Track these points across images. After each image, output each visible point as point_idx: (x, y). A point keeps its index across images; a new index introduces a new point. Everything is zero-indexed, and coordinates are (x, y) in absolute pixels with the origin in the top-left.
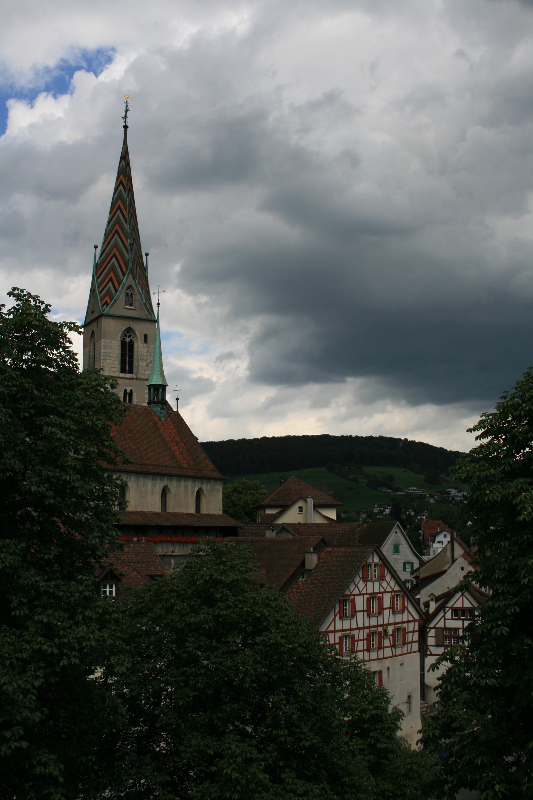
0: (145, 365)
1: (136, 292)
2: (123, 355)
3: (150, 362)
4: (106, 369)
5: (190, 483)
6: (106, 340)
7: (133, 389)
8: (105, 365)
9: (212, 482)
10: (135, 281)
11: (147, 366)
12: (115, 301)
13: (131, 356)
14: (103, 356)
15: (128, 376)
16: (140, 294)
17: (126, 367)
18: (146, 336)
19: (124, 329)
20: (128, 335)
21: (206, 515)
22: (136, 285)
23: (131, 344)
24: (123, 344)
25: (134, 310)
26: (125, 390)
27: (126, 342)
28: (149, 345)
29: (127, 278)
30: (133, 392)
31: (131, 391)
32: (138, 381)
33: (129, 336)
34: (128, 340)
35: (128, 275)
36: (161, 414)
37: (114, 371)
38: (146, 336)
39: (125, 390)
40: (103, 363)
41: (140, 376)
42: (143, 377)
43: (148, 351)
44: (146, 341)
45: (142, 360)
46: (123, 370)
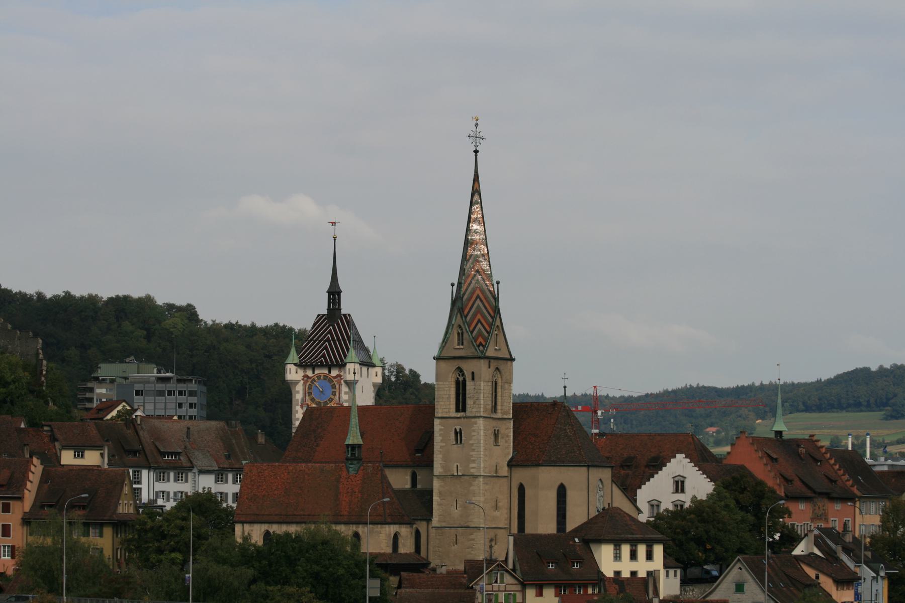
1: (464, 331)
3: (477, 400)
4: (440, 410)
15: (459, 415)
23: (464, 381)
24: (457, 382)
26: (456, 429)
27: (459, 381)
31: (460, 429)
32: (465, 419)
34: (461, 379)
35: (457, 314)
39: (456, 429)
41: (468, 414)
42: (471, 415)
43: (475, 388)
44: (473, 379)
46: (457, 410)
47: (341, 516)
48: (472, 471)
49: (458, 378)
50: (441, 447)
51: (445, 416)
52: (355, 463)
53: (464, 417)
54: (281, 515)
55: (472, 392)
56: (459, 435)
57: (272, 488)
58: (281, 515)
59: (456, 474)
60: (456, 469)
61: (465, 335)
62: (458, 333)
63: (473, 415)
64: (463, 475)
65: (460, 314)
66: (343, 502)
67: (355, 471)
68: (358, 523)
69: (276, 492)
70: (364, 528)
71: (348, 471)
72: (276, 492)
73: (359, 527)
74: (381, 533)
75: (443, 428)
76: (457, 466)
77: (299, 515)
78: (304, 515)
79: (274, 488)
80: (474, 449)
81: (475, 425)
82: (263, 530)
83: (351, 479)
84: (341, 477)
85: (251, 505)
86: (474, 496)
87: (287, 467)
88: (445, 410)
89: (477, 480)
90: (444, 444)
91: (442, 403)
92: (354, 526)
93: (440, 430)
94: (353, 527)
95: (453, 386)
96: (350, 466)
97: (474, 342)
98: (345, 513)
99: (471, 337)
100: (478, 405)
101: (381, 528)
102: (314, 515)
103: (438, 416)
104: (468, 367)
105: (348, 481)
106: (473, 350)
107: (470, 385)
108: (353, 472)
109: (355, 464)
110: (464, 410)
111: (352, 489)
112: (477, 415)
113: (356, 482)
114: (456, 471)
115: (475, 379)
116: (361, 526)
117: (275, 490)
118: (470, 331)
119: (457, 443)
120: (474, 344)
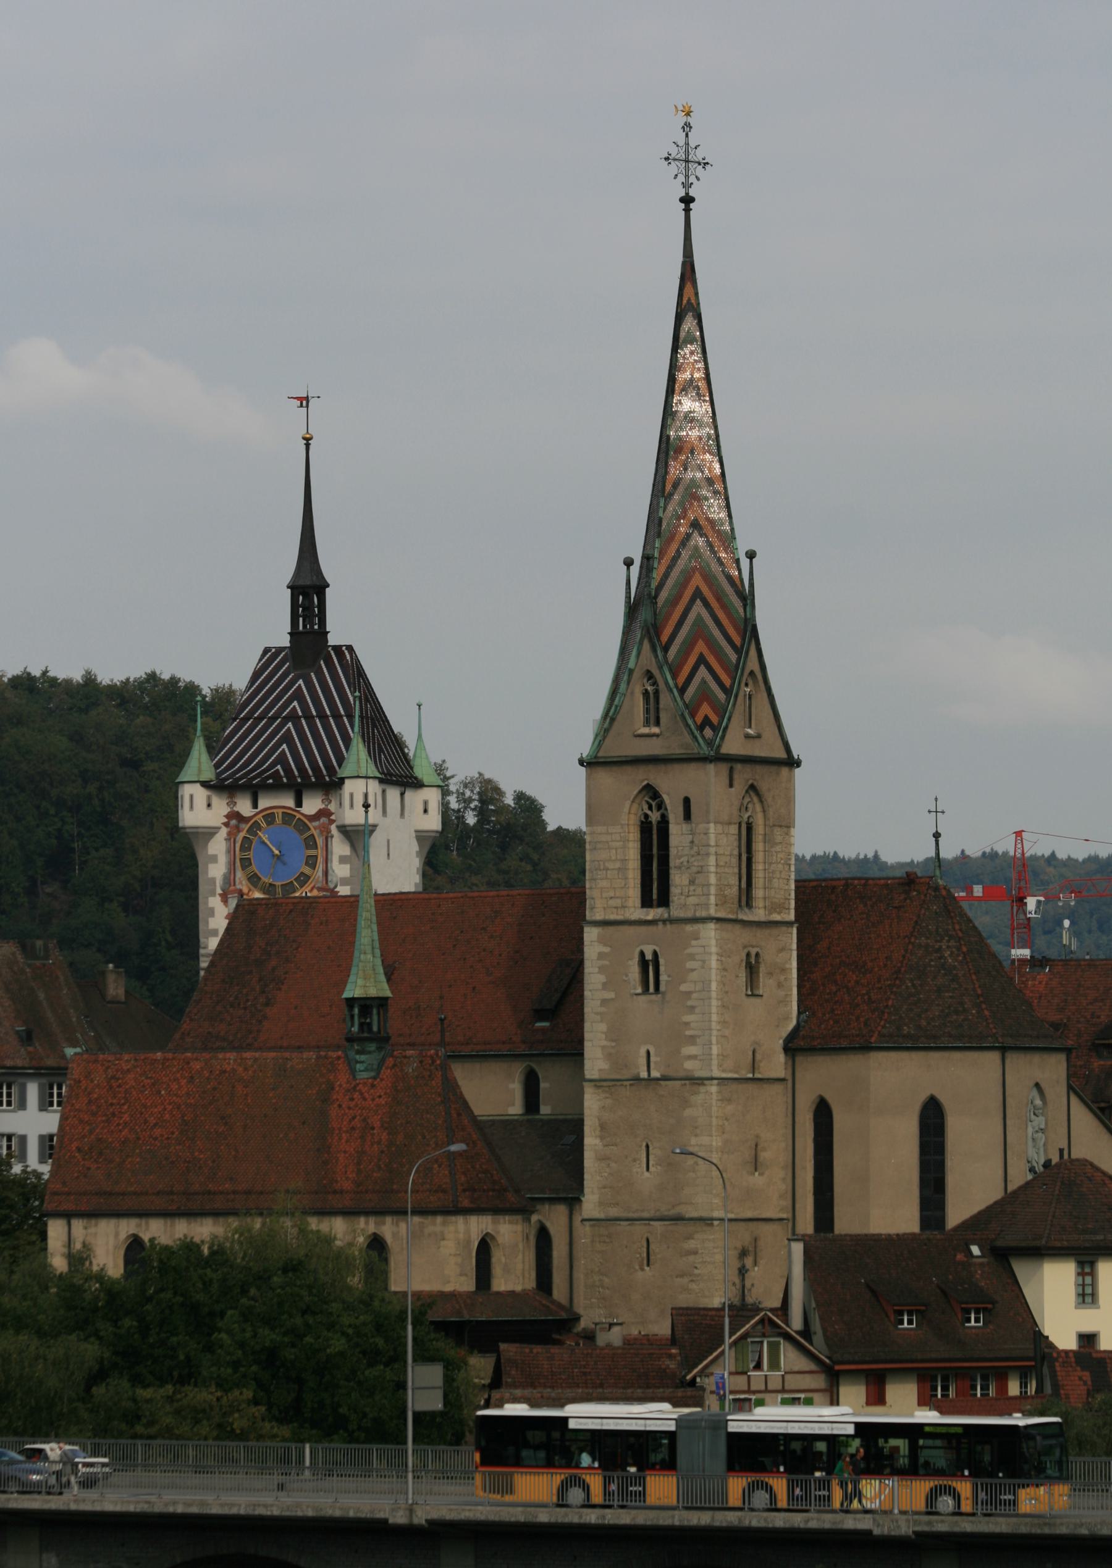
3: (698, 872)
11: (692, 882)
16: (671, 691)
19: (635, 793)
22: (660, 668)
25: (657, 736)
26: (642, 954)
34: (655, 817)
37: (616, 908)
43: (692, 842)
46: (646, 902)
47: (335, 1192)
48: (689, 1065)
50: (604, 1002)
53: (664, 921)
54: (172, 1193)
57: (146, 1122)
59: (644, 1074)
60: (643, 1061)
63: (689, 914)
64: (665, 1078)
67: (372, 1070)
68: (380, 1212)
69: (157, 1132)
72: (157, 1132)
73: (384, 1223)
74: (444, 1239)
75: (607, 950)
76: (648, 1053)
79: (152, 1120)
80: (693, 1007)
81: (694, 943)
82: (123, 1236)
83: (362, 1094)
84: (333, 1089)
86: (696, 1135)
87: (188, 1063)
90: (612, 995)
93: (601, 956)
98: (347, 1185)
99: (680, 703)
105: (352, 1099)
106: (688, 739)
109: (370, 1053)
111: (365, 1120)
112: (698, 914)
113: (373, 1100)
115: (693, 817)
116: (389, 1219)
117: (155, 1125)
118: (676, 686)
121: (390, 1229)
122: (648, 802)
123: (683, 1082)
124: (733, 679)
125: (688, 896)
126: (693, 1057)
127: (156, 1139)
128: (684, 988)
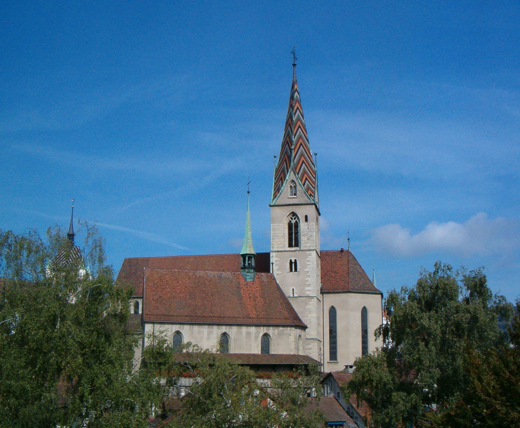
0: (306, 239)
1: (297, 184)
2: (290, 234)
4: (275, 246)
5: (253, 329)
6: (274, 224)
7: (296, 259)
8: (274, 243)
9: (281, 328)
10: (295, 176)
11: (308, 239)
12: (281, 194)
13: (297, 233)
14: (273, 237)
15: (293, 249)
17: (292, 243)
18: (306, 217)
19: (288, 214)
20: (293, 218)
21: (273, 355)
23: (297, 225)
24: (290, 225)
25: (296, 198)
26: (291, 261)
28: (309, 223)
29: (289, 175)
30: (297, 261)
31: (295, 260)
32: (300, 252)
33: (295, 219)
34: (293, 222)
35: (290, 172)
36: (247, 277)
38: (306, 217)
39: (291, 261)
40: (273, 241)
41: (302, 248)
43: (308, 228)
44: (306, 220)
45: (304, 235)
46: (290, 245)
47: (250, 318)
48: (308, 293)
49: (290, 221)
51: (280, 250)
52: (252, 271)
53: (299, 251)
54: (191, 316)
55: (306, 230)
56: (293, 265)
57: (176, 292)
58: (191, 316)
59: (292, 296)
60: (292, 291)
61: (299, 188)
62: (291, 187)
63: (307, 249)
65: (294, 171)
66: (249, 307)
70: (274, 330)
71: (246, 279)
76: (293, 289)
77: (210, 317)
78: (214, 317)
81: (309, 257)
84: (240, 284)
85: (158, 306)
88: (282, 246)
89: (313, 300)
90: (281, 272)
91: (278, 240)
92: (265, 328)
94: (263, 329)
95: (287, 227)
96: (247, 274)
97: (306, 193)
98: (254, 316)
100: (312, 240)
101: (290, 330)
102: (224, 317)
103: (274, 250)
104: (301, 212)
106: (307, 198)
107: (303, 226)
108: (249, 280)
109: (251, 273)
110: (297, 245)
112: (310, 249)
114: (292, 294)
116: (271, 328)
119: (291, 270)
120: (307, 194)
121: (272, 331)
122: (291, 217)
123: (306, 298)
124: (315, 185)
125: (307, 243)
126: (308, 290)
127: (181, 297)
128: (306, 270)
